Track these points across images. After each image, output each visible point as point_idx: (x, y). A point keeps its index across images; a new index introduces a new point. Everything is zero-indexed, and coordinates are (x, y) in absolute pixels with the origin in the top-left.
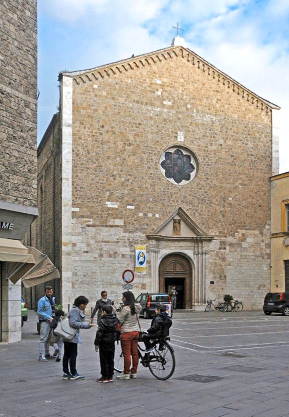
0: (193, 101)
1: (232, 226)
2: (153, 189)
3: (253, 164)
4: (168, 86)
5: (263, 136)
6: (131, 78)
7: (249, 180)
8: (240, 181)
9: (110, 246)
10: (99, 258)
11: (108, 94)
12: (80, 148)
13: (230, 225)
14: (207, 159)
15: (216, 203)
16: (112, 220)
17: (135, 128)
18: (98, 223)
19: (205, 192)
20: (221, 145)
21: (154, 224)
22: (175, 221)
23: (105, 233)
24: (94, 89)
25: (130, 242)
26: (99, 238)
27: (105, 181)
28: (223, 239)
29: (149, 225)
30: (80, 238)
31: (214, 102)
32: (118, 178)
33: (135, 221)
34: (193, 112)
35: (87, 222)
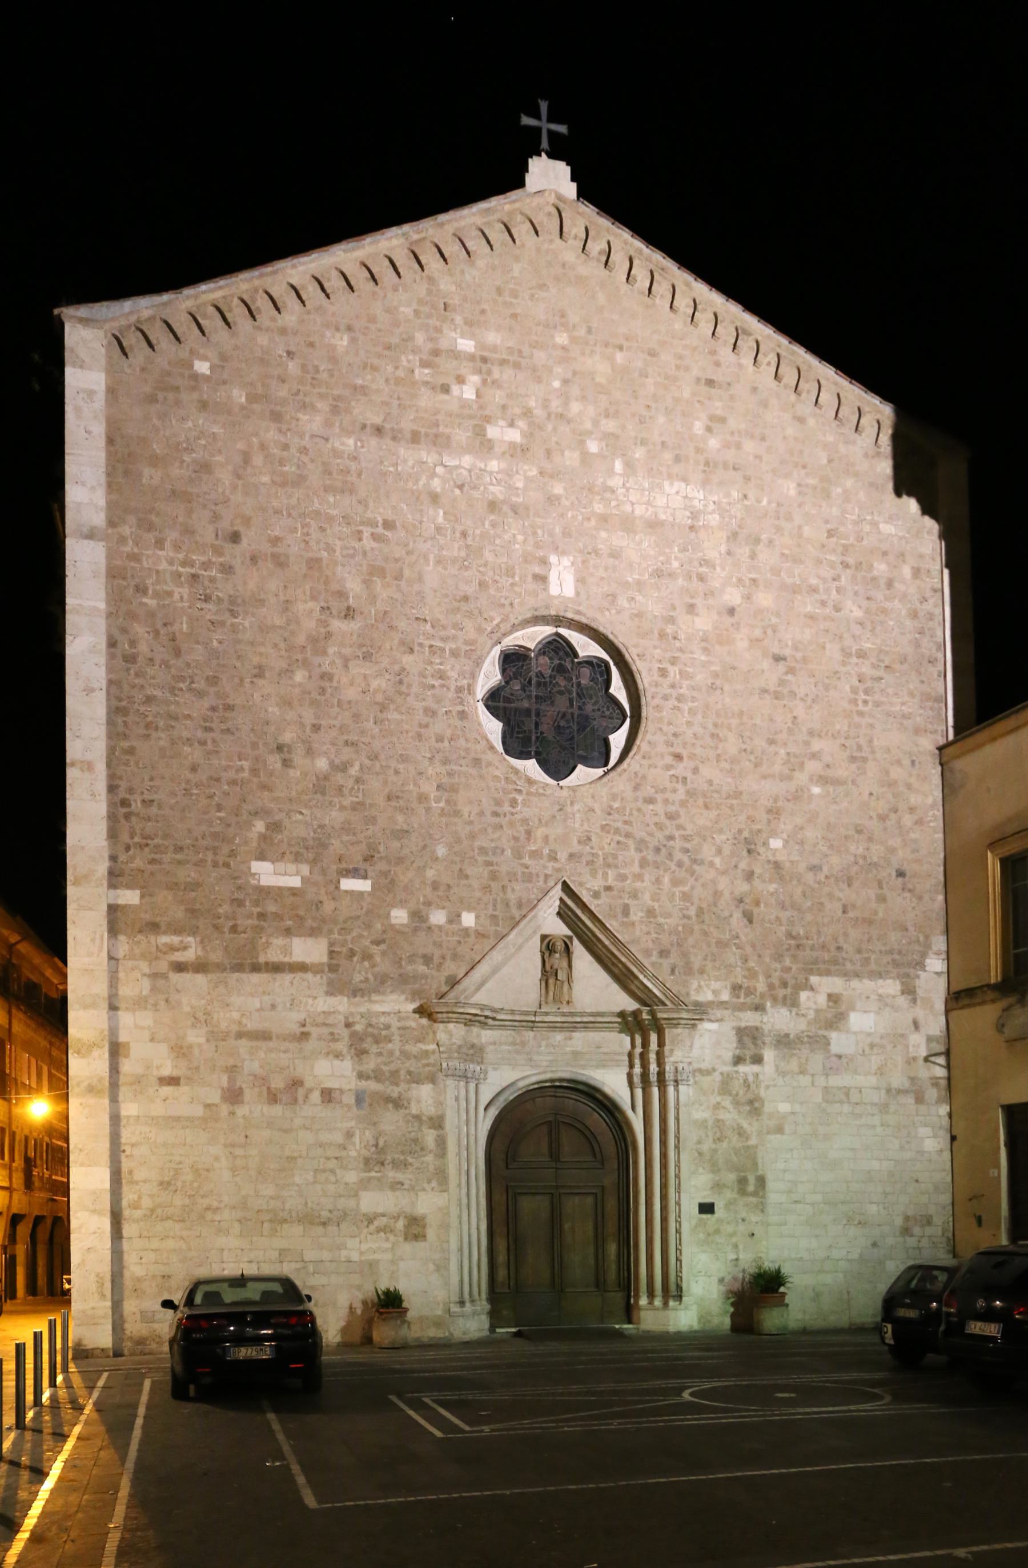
0: (610, 425)
1: (787, 962)
2: (448, 802)
3: (866, 692)
4: (503, 362)
5: (907, 571)
6: (349, 328)
7: (853, 759)
8: (813, 767)
9: (273, 1055)
10: (225, 1109)
11: (252, 398)
12: (140, 630)
13: (778, 957)
14: (673, 671)
15: (717, 861)
16: (279, 941)
17: (368, 543)
18: (216, 956)
19: (671, 817)
20: (731, 611)
21: (455, 957)
23: (248, 999)
24: (195, 377)
25: (354, 1035)
26: (225, 1019)
27: (246, 775)
28: (750, 1019)
29: (436, 960)
30: (146, 1018)
31: (698, 427)
32: (298, 758)
33: (377, 943)
34: (611, 472)
35: (173, 949)
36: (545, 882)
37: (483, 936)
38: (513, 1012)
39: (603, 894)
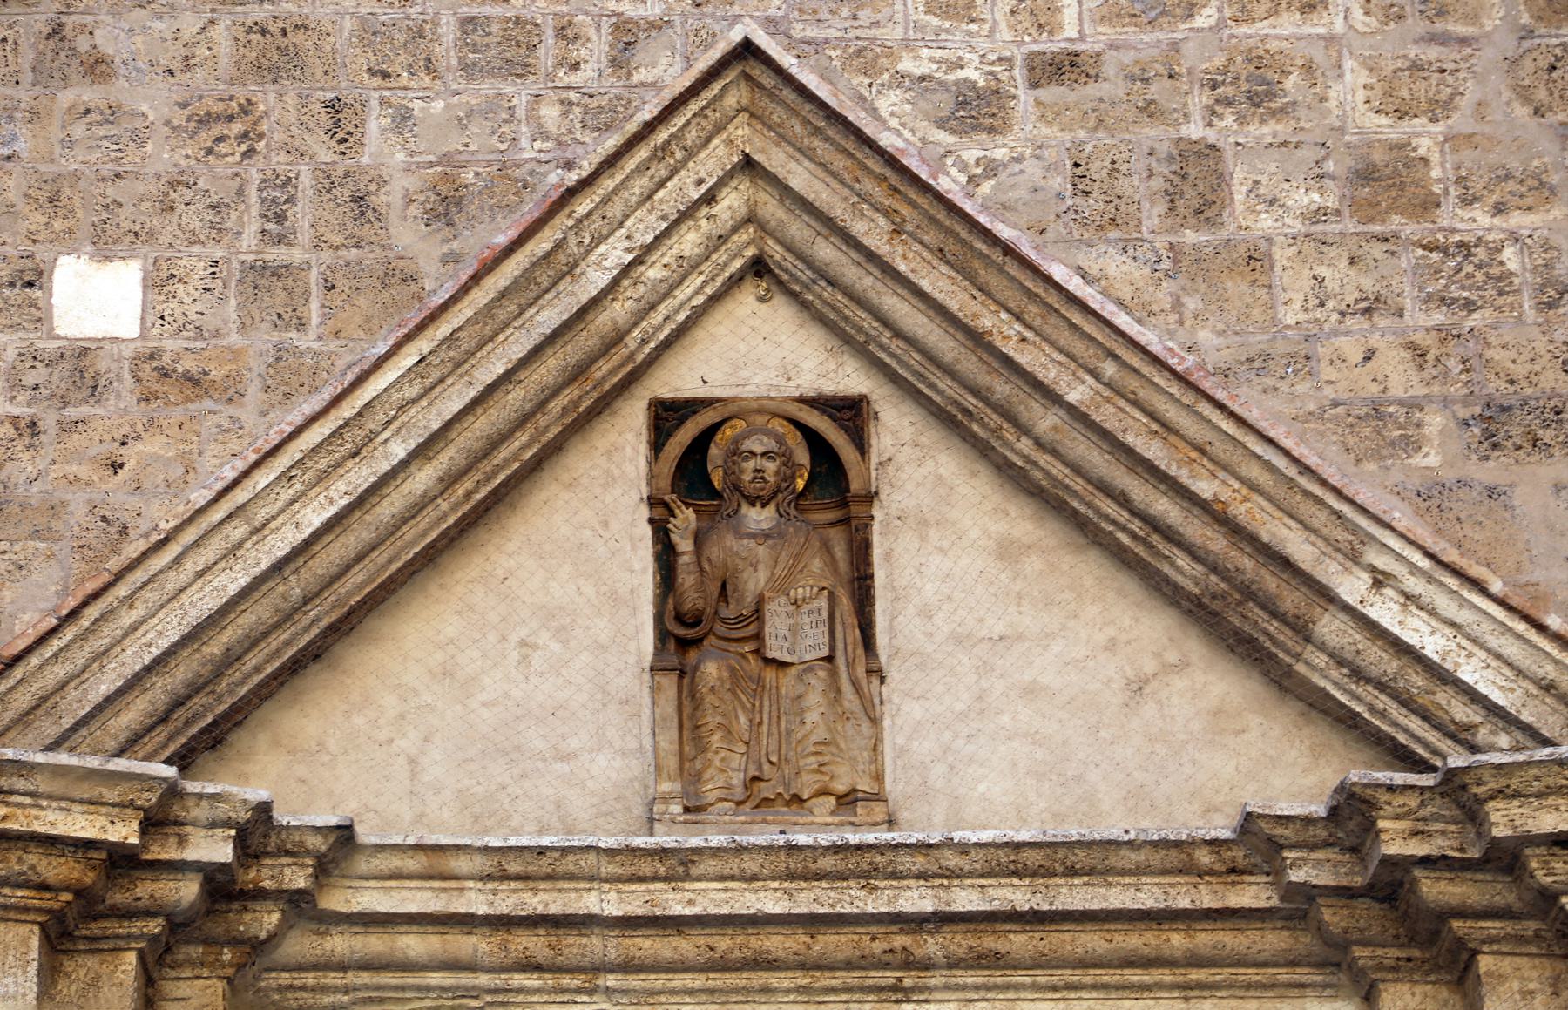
22: (695, 462)
36: (620, 61)
37: (195, 383)
38: (434, 862)
39: (1024, 98)
